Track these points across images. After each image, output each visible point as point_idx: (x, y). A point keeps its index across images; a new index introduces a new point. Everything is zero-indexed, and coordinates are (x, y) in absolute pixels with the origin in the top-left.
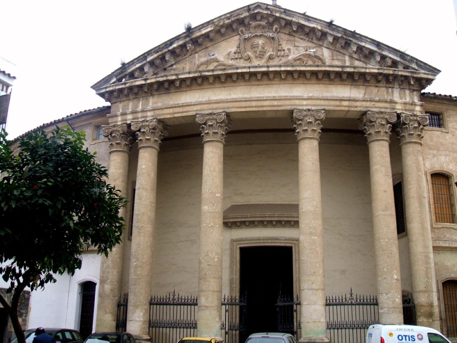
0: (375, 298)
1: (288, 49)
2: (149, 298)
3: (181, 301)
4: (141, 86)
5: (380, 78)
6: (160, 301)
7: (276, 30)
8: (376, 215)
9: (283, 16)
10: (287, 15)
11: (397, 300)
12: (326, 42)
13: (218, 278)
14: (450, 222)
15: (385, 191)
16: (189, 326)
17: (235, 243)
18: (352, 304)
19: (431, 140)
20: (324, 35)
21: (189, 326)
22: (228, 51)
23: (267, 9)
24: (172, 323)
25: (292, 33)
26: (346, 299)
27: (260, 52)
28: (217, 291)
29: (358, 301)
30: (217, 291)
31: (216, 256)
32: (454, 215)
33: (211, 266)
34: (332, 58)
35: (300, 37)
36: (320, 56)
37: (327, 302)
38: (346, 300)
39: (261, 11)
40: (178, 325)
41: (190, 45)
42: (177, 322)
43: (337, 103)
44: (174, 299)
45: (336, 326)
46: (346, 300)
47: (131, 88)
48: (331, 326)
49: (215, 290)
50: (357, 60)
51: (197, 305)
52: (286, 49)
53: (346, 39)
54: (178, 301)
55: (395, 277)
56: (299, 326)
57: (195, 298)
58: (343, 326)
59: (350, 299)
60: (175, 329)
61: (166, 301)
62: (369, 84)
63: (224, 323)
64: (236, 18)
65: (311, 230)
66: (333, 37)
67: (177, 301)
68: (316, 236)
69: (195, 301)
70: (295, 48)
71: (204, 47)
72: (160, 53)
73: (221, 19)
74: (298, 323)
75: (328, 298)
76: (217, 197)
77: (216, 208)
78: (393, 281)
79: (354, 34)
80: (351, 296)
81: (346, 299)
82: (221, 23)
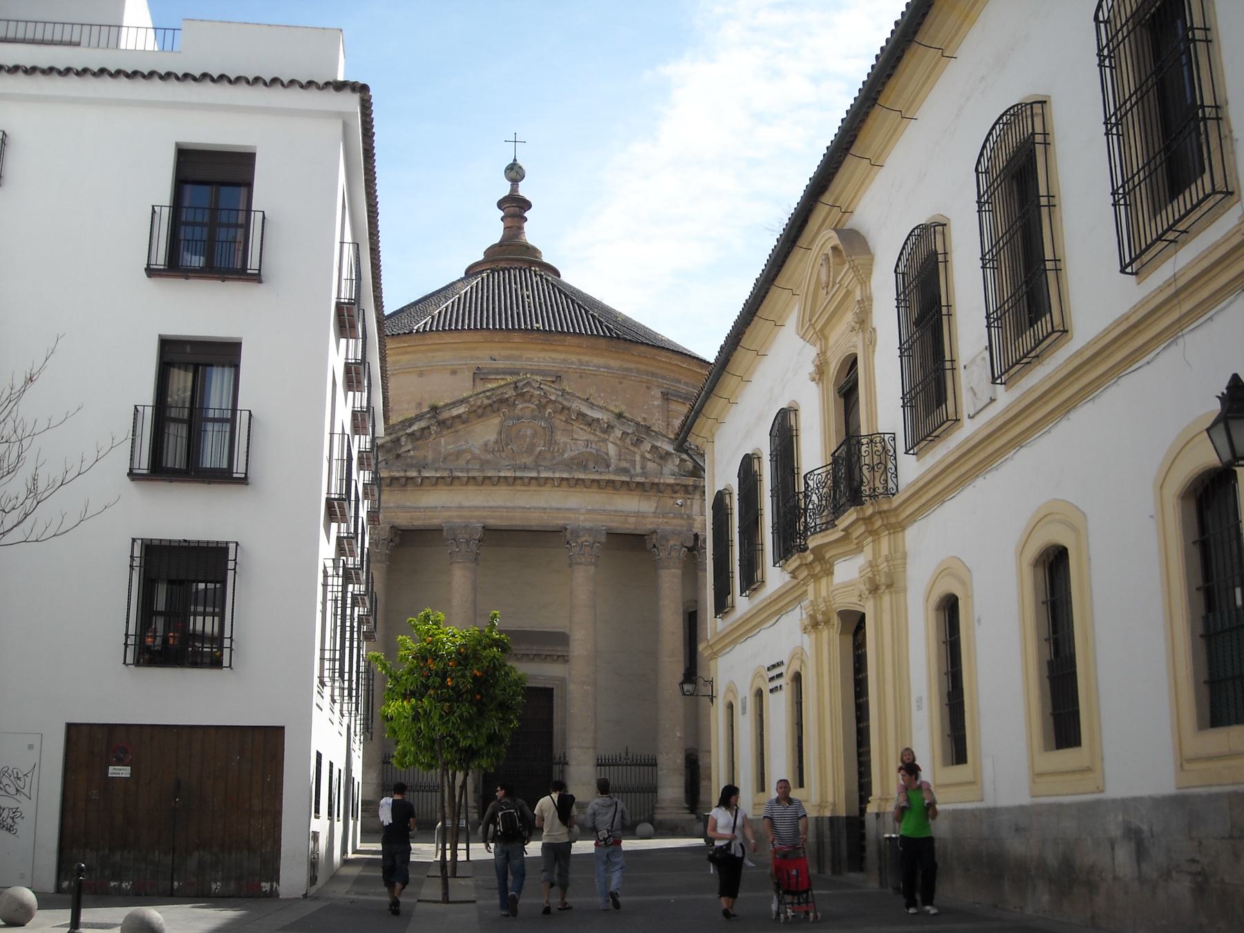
5: (678, 487)
9: (560, 399)
10: (566, 399)
15: (673, 633)
18: (627, 765)
26: (620, 758)
29: (635, 761)
34: (618, 458)
38: (620, 760)
41: (435, 428)
46: (620, 760)
55: (678, 734)
62: (662, 495)
71: (453, 430)
73: (479, 398)
75: (600, 758)
80: (627, 755)
81: (620, 758)
82: (479, 403)
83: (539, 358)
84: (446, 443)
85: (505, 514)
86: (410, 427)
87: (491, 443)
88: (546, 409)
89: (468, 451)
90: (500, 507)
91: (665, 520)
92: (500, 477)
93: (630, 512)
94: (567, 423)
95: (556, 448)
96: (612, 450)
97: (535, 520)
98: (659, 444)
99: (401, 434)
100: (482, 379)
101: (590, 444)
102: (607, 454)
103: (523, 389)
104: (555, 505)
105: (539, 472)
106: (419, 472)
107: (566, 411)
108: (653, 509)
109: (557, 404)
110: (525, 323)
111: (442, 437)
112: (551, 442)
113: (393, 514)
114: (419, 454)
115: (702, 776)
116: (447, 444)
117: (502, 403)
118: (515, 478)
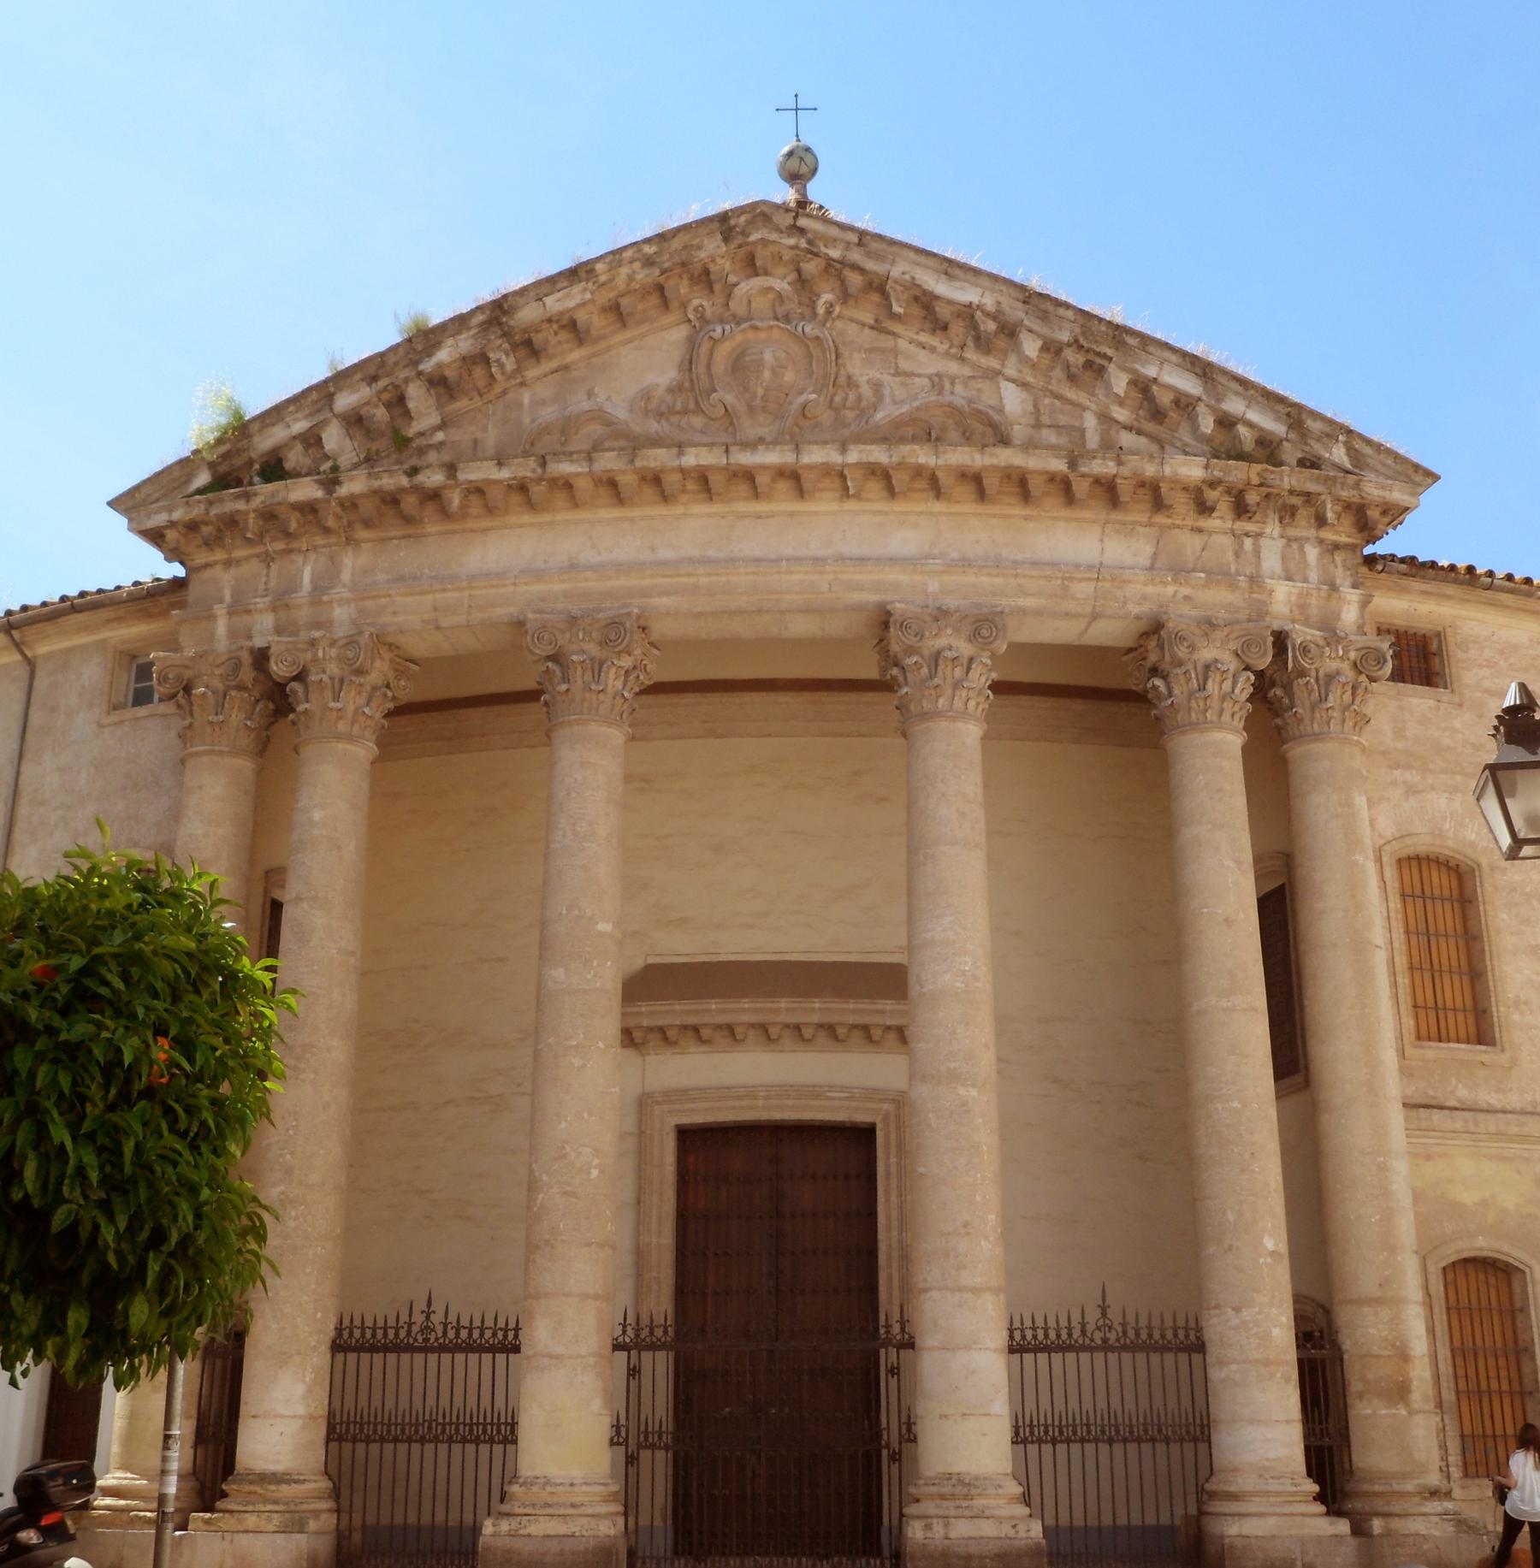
0: (1192, 1324)
2: (332, 1327)
3: (457, 1335)
4: (309, 509)
6: (374, 1336)
8: (1195, 1008)
9: (856, 256)
10: (868, 255)
11: (1276, 1332)
12: (1012, 360)
13: (602, 1246)
14: (1468, 1042)
16: (485, 1431)
18: (1106, 1347)
19: (1399, 733)
21: (485, 1431)
24: (421, 1420)
26: (1083, 1325)
27: (766, 390)
28: (596, 1297)
29: (1131, 1334)
30: (596, 1297)
31: (596, 1162)
32: (1485, 1012)
33: (574, 1200)
34: (1032, 421)
35: (915, 337)
36: (991, 412)
37: (1011, 1337)
40: (443, 1431)
42: (440, 1420)
44: (427, 1327)
45: (1046, 1432)
46: (1083, 1332)
47: (269, 516)
48: (1027, 1429)
49: (591, 1291)
50: (1129, 428)
51: (517, 1349)
52: (863, 380)
53: (1088, 351)
54: (445, 1333)
55: (1269, 1244)
56: (909, 1430)
57: (512, 1325)
58: (1075, 1433)
59: (1098, 1328)
60: (429, 1447)
61: (397, 1335)
62: (1169, 521)
63: (623, 1422)
65: (952, 1065)
66: (1039, 343)
67: (440, 1334)
68: (973, 1085)
69: (511, 1335)
70: (898, 379)
74: (904, 1419)
75: (1017, 1324)
76: (601, 934)
77: (595, 976)
78: (1262, 1260)
79: (1119, 333)
80: (1104, 1315)
81: (1083, 1325)
85: (703, 580)
86: (430, 355)
87: (660, 392)
88: (818, 296)
89: (600, 416)
90: (690, 560)
91: (1185, 591)
93: (1077, 566)
95: (852, 397)
96: (1013, 401)
98: (1151, 371)
99: (403, 374)
101: (947, 386)
102: (1000, 410)
103: (748, 235)
104: (852, 548)
105: (798, 450)
106: (451, 469)
107: (875, 297)
108: (1144, 560)
109: (848, 273)
112: (835, 381)
113: (384, 601)
114: (460, 435)
115: (1355, 1386)
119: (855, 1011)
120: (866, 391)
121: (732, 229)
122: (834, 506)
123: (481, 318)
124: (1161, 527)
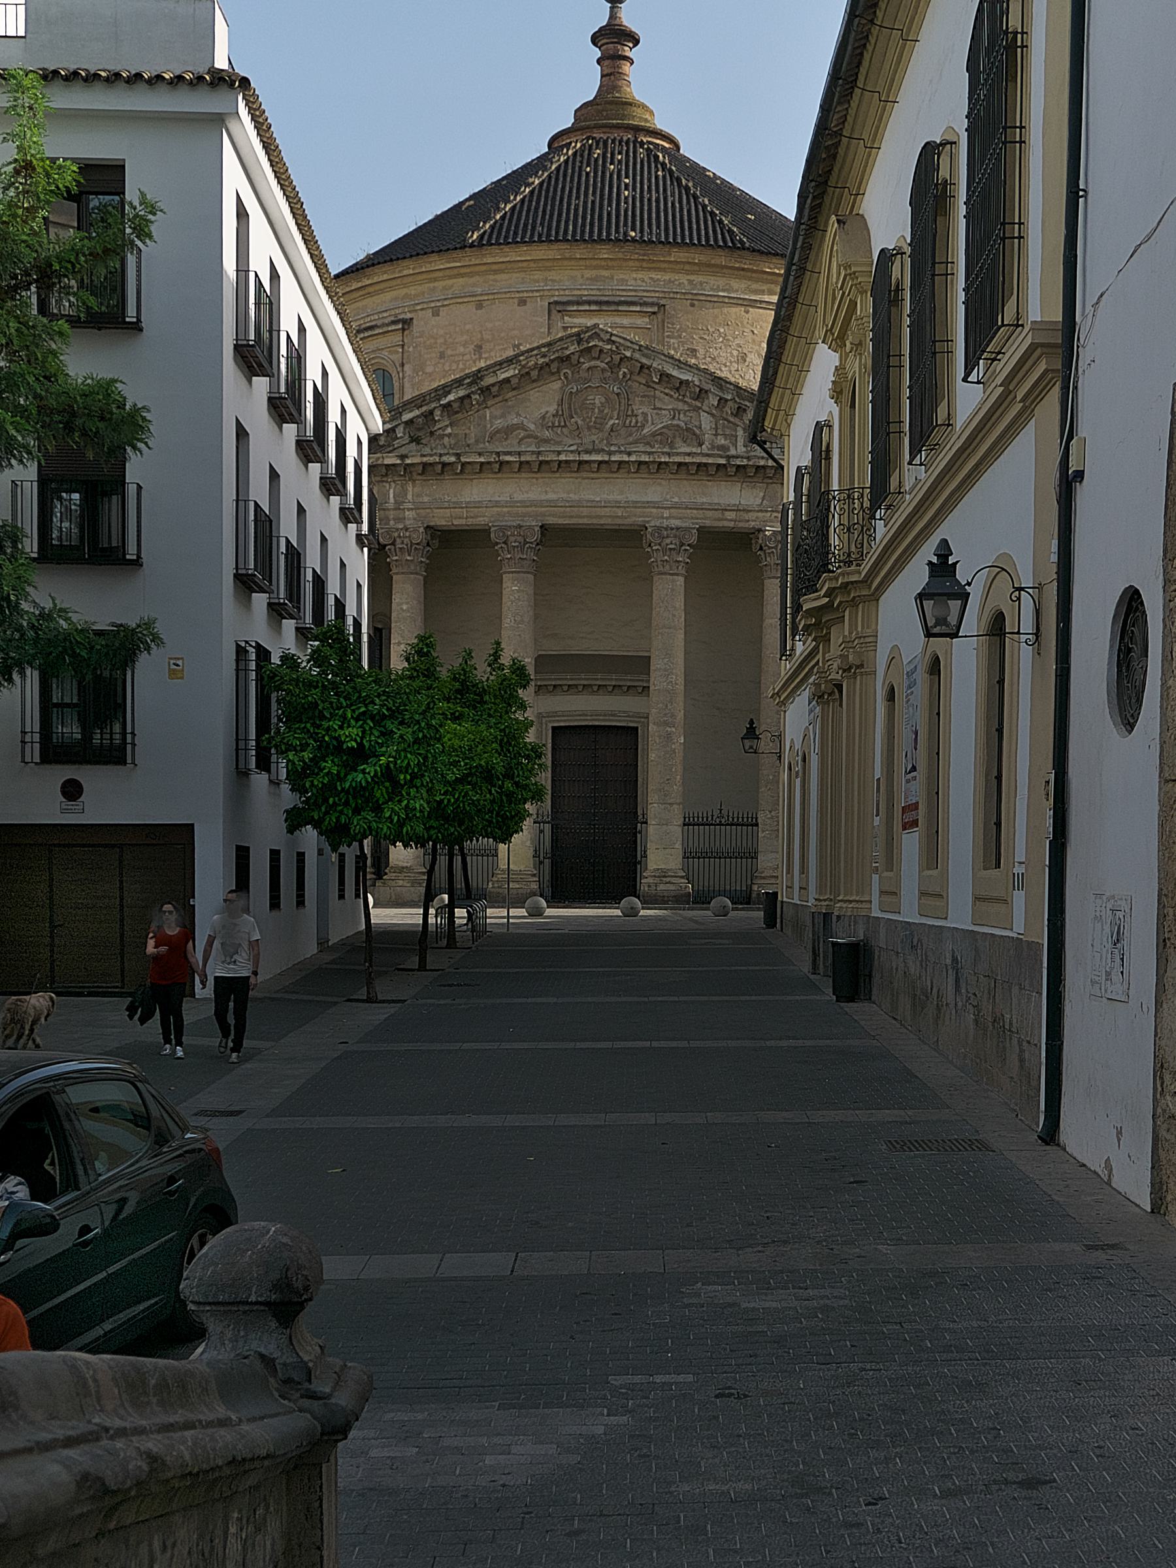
1: (643, 413)
7: (624, 377)
9: (637, 355)
10: (643, 355)
17: (544, 720)
18: (720, 824)
20: (702, 394)
22: (543, 411)
23: (610, 341)
25: (651, 384)
26: (712, 816)
39: (600, 344)
43: (718, 514)
64: (557, 355)
71: (500, 398)
72: (424, 409)
81: (712, 816)
83: (636, 279)
84: (494, 417)
86: (445, 397)
89: (521, 427)
92: (560, 462)
94: (649, 386)
95: (634, 421)
97: (606, 518)
100: (559, 311)
110: (617, 231)
111: (486, 407)
113: (428, 511)
116: (493, 417)
117: (563, 361)
118: (581, 463)
119: (630, 680)
120: (640, 419)
121: (581, 339)
122: (626, 475)
123: (468, 381)
124: (767, 483)
